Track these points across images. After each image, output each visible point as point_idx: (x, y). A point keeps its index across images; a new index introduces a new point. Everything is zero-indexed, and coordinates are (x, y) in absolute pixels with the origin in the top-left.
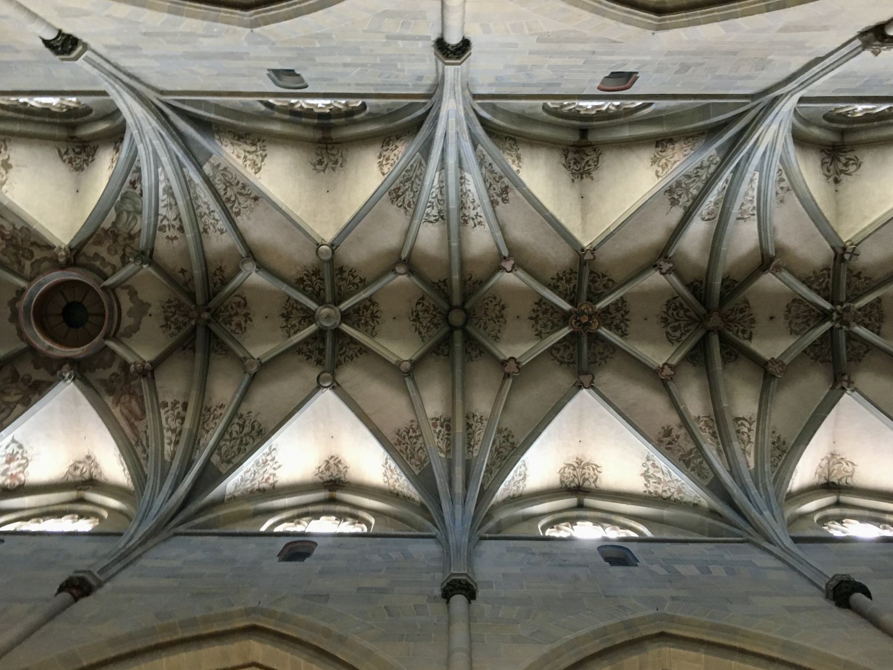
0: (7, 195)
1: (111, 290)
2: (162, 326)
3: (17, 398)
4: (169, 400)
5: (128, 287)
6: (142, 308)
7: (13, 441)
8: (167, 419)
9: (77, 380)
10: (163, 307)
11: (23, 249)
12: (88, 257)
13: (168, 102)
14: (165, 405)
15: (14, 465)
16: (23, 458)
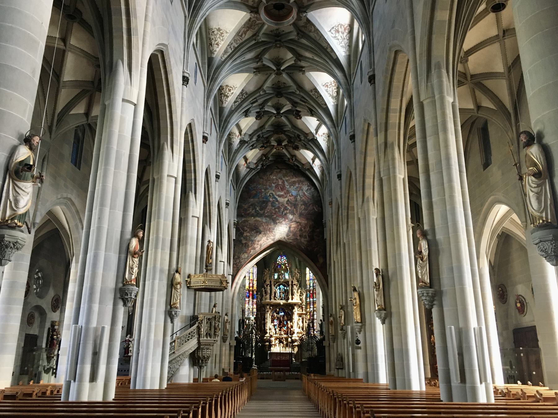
7: (330, 31)
11: (252, 23)
12: (254, 4)
13: (187, 9)
15: (340, 30)
16: (338, 26)
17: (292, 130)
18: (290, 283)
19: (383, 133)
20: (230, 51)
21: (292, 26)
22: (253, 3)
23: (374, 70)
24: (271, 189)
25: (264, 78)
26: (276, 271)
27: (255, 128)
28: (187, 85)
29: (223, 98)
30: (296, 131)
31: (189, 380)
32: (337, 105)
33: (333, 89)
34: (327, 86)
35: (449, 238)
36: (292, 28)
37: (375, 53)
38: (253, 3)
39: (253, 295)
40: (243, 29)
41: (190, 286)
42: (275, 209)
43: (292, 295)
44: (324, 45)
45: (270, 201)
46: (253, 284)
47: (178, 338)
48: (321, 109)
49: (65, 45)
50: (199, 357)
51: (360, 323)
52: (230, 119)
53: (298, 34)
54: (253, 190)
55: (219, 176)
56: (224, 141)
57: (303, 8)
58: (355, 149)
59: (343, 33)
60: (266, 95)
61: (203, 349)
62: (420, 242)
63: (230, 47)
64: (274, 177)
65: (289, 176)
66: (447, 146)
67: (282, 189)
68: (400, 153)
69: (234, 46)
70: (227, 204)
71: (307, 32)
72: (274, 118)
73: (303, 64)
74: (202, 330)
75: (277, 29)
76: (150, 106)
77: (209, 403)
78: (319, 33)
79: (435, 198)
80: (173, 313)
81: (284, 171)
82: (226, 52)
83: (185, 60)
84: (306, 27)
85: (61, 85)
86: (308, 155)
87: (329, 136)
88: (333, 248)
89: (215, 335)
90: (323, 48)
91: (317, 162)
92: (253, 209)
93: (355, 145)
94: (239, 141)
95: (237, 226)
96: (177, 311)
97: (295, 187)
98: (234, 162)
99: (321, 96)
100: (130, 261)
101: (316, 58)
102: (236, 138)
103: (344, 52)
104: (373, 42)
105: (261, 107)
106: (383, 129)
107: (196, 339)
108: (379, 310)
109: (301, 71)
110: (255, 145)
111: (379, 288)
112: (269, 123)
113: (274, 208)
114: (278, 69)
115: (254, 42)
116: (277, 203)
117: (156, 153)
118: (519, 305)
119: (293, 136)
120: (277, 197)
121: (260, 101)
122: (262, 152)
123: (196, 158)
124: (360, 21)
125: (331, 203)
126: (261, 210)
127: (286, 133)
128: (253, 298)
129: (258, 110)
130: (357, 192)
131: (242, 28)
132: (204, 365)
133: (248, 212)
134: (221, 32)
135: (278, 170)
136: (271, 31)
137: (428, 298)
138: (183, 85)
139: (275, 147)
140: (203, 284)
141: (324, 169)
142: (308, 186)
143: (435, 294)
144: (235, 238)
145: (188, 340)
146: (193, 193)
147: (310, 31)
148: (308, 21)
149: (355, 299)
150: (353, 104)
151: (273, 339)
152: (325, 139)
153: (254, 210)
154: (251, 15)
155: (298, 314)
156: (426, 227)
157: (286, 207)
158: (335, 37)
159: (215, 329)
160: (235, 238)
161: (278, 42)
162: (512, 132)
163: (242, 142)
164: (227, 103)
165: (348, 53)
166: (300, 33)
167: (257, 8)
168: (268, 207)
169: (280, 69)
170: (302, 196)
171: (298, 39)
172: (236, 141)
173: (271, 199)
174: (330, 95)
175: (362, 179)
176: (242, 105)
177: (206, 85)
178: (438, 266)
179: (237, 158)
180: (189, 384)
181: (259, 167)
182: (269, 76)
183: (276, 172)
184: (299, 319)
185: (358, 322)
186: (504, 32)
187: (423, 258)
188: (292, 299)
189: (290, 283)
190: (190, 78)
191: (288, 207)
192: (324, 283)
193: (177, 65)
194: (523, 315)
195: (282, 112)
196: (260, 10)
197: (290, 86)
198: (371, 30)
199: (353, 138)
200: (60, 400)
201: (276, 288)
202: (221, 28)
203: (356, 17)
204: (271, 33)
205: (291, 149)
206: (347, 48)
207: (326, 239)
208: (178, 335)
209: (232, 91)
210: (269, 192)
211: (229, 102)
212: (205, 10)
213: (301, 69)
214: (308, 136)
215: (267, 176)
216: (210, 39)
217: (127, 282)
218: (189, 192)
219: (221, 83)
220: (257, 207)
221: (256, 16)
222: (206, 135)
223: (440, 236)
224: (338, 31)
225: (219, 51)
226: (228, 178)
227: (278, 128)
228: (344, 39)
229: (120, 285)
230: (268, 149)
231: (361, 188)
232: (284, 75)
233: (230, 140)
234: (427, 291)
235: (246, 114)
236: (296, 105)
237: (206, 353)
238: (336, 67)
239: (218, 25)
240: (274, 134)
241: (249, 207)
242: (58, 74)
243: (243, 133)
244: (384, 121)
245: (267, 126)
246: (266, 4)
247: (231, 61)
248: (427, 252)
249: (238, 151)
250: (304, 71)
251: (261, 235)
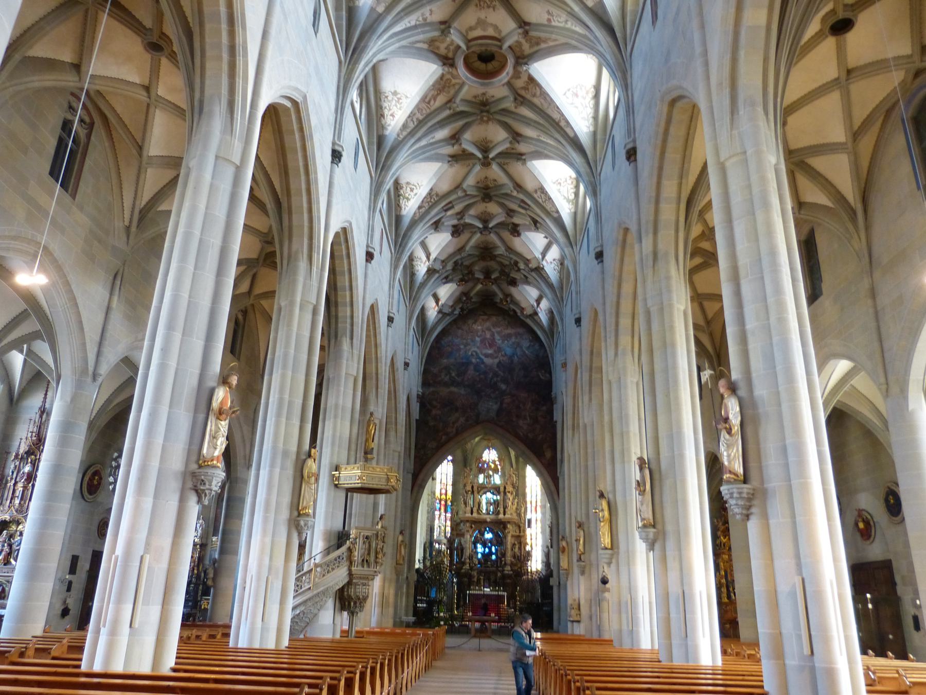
0: (413, 95)
1: (468, 41)
2: (494, 10)
4: (546, 16)
5: (467, 32)
6: (481, 23)
7: (565, 94)
8: (559, 22)
9: (529, 63)
10: (481, 9)
14: (549, 20)
17: (506, 254)
18: (502, 489)
19: (651, 236)
20: (412, 126)
21: (505, 86)
22: (446, 51)
23: (634, 141)
24: (474, 345)
25: (465, 170)
26: (481, 470)
27: (451, 250)
28: (340, 165)
29: (401, 202)
30: (511, 256)
31: (334, 634)
32: (575, 214)
33: (568, 190)
34: (560, 184)
35: (778, 393)
36: (504, 92)
37: (636, 112)
38: (446, 51)
39: (446, 505)
40: (432, 92)
41: (338, 484)
42: (479, 375)
43: (505, 508)
44: (556, 116)
45: (471, 363)
46: (446, 491)
47: (316, 566)
48: (550, 220)
49: (149, 97)
50: (350, 596)
51: (610, 549)
52: (411, 234)
53: (515, 99)
54: (449, 346)
55: (393, 318)
56: (401, 267)
57: (522, 59)
58: (603, 273)
59: (584, 98)
60: (467, 198)
61: (356, 584)
62: (725, 401)
63: (412, 120)
64: (479, 328)
66: (770, 233)
67: (491, 346)
68: (678, 269)
69: (417, 119)
70: (407, 365)
71: (528, 96)
72: (478, 235)
73: (522, 148)
74: (356, 554)
75: (484, 94)
76: (279, 193)
77: (346, 679)
78: (548, 98)
79: (751, 324)
80: (302, 523)
81: (494, 319)
82: (405, 126)
83: (337, 126)
84: (528, 89)
85: (144, 163)
86: (528, 294)
87: (562, 264)
88: (568, 433)
89: (376, 562)
90: (554, 120)
91: (544, 304)
92: (446, 375)
93: (603, 267)
94: (426, 269)
95: (422, 399)
96: (308, 521)
98: (417, 301)
99: (550, 198)
100: (211, 426)
101: (544, 138)
102: (422, 265)
103: (587, 126)
104: (633, 100)
105: (459, 217)
106: (651, 230)
107: (346, 568)
108: (645, 526)
109: (518, 159)
110: (450, 277)
111: (645, 490)
112: (473, 242)
114: (486, 158)
115: (447, 113)
116: (482, 366)
117: (285, 262)
118: (861, 525)
119: (507, 263)
120: (483, 357)
121: (458, 208)
122: (461, 289)
123: (354, 284)
124: (612, 70)
125: (564, 365)
126: (458, 375)
127: (498, 259)
128: (446, 511)
129: (455, 222)
130: (606, 341)
131: (429, 90)
132: (357, 610)
133: (440, 379)
134: (399, 96)
135: (486, 317)
136: (475, 97)
137: (741, 502)
138: (332, 162)
139: (481, 281)
140: (359, 481)
141: (555, 313)
142: (531, 341)
143: (753, 494)
144: (418, 418)
145: (333, 569)
146: (348, 339)
147: (534, 95)
148: (531, 79)
149: (602, 510)
150: (600, 203)
151: (475, 573)
152: (556, 267)
153: (448, 377)
154: (443, 70)
155: (512, 536)
156: (735, 375)
158: (572, 104)
159: (377, 553)
160: (418, 418)
161: (485, 114)
162: (858, 240)
163: (431, 272)
164: (407, 209)
165: (592, 129)
166: (518, 98)
167: (453, 59)
168: (469, 372)
169: (488, 157)
171: (516, 108)
172: (422, 268)
173: (474, 360)
174: (565, 198)
175: (613, 320)
176: (429, 213)
177: (373, 175)
178: (758, 444)
179: (423, 296)
180: (333, 641)
181: (457, 312)
182: (471, 169)
183: (483, 320)
184: (514, 544)
185: (606, 549)
186: (849, 72)
187: (731, 429)
188: (504, 514)
189: (502, 489)
190: (344, 154)
191: (500, 372)
192: (553, 488)
193: (322, 129)
194: (868, 542)
195: (491, 225)
196: (456, 60)
197: (502, 185)
198: (629, 81)
199: (599, 256)
200: (79, 667)
201: (481, 496)
202: (398, 91)
203: (605, 64)
204: (474, 100)
205: (504, 285)
206: (591, 120)
207: (556, 422)
208: (317, 561)
209: (415, 191)
210: (469, 350)
211: (410, 206)
212: (371, 54)
213: (520, 157)
214: (530, 263)
215: (469, 325)
216: (381, 108)
217: (205, 462)
218: (341, 337)
219: (397, 174)
221: (451, 70)
222: (370, 250)
223: (761, 391)
224: (577, 95)
225: (395, 125)
226: (409, 325)
227: (486, 252)
228: (586, 107)
229: (194, 467)
230: (470, 284)
231: (613, 334)
232: (494, 166)
233: (413, 268)
234: (738, 488)
235: (437, 226)
236: (512, 214)
237: (360, 590)
238: (574, 150)
239: (395, 87)
240: (479, 260)
242: (138, 137)
243: (433, 257)
244: (652, 218)
245: (467, 248)
246: (467, 52)
247: (413, 141)
248: (739, 418)
249: (423, 284)
250: (525, 160)
251: (457, 415)
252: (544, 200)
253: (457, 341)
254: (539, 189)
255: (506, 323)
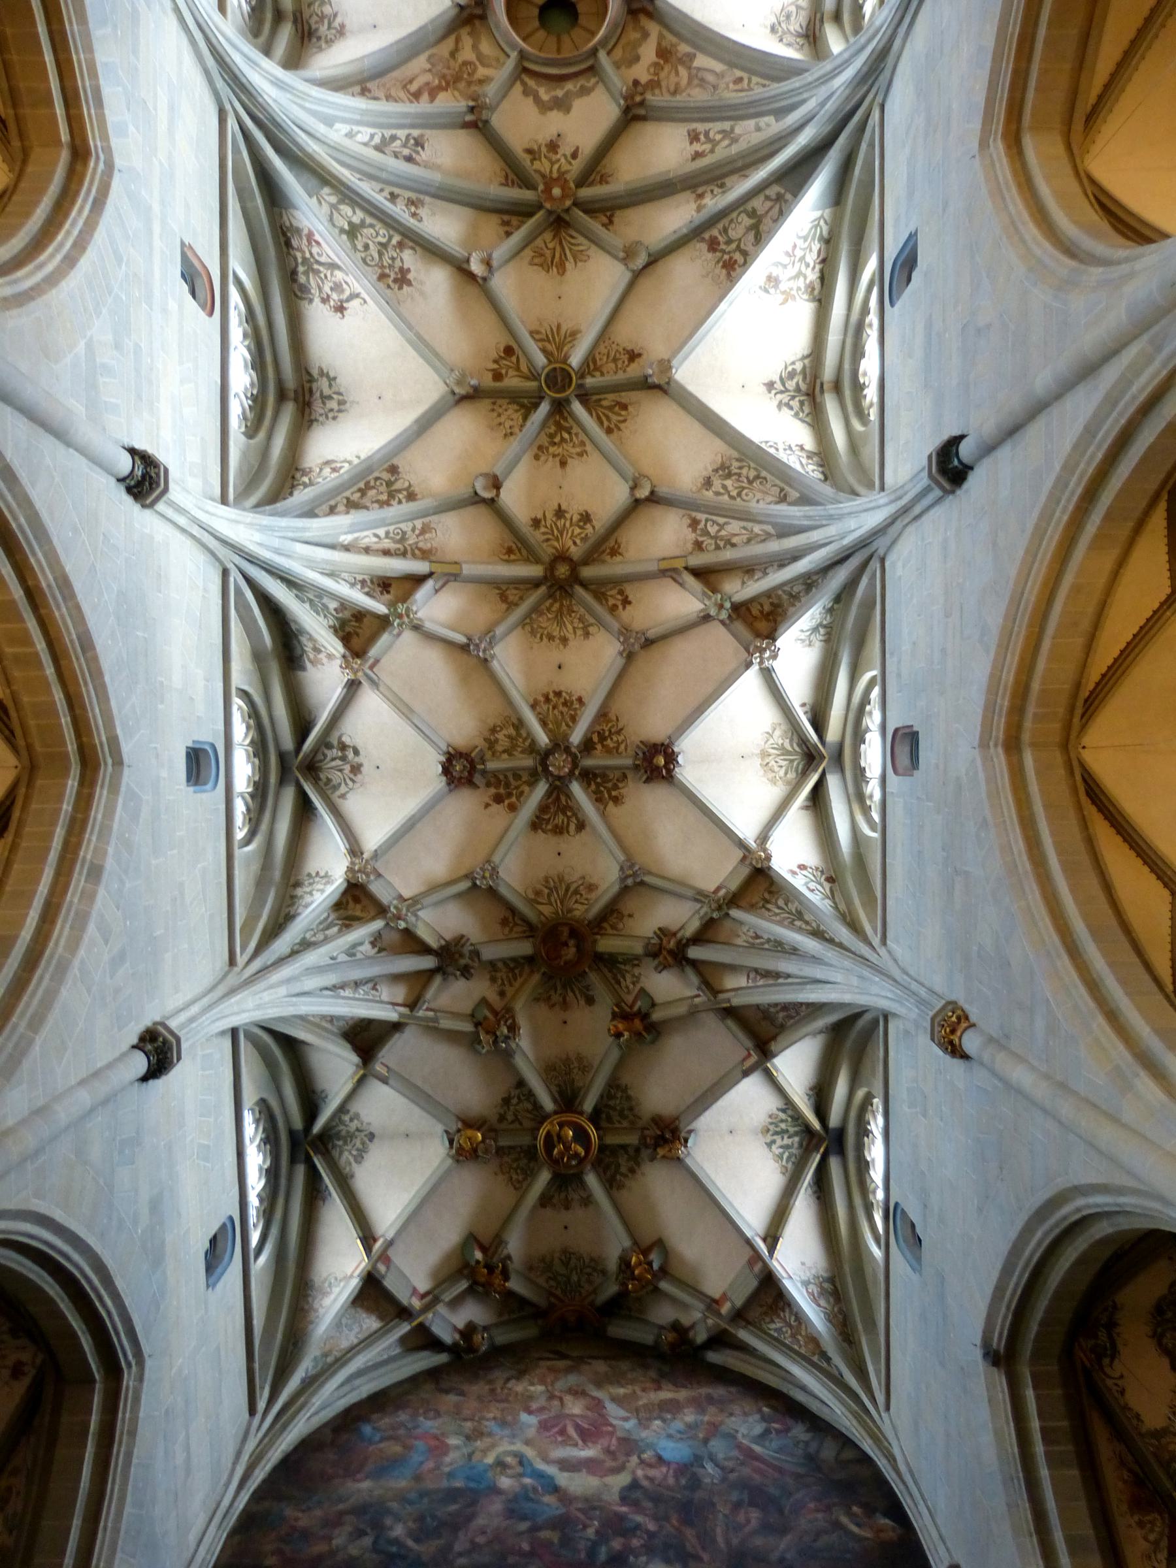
3: (683, 72)
42: (535, 1529)
65: (632, 1382)
92: (361, 1533)
97: (678, 1425)
113: (524, 1526)
116: (548, 1499)
142: (764, 1418)
153: (367, 1541)
157: (621, 1518)
168: (480, 1521)
170: (730, 1464)
173: (505, 1482)
191: (639, 1518)
220: (398, 1518)
241: (335, 1521)
252: (734, 493)
253: (429, 1425)
254: (716, 471)
255: (653, 1374)
